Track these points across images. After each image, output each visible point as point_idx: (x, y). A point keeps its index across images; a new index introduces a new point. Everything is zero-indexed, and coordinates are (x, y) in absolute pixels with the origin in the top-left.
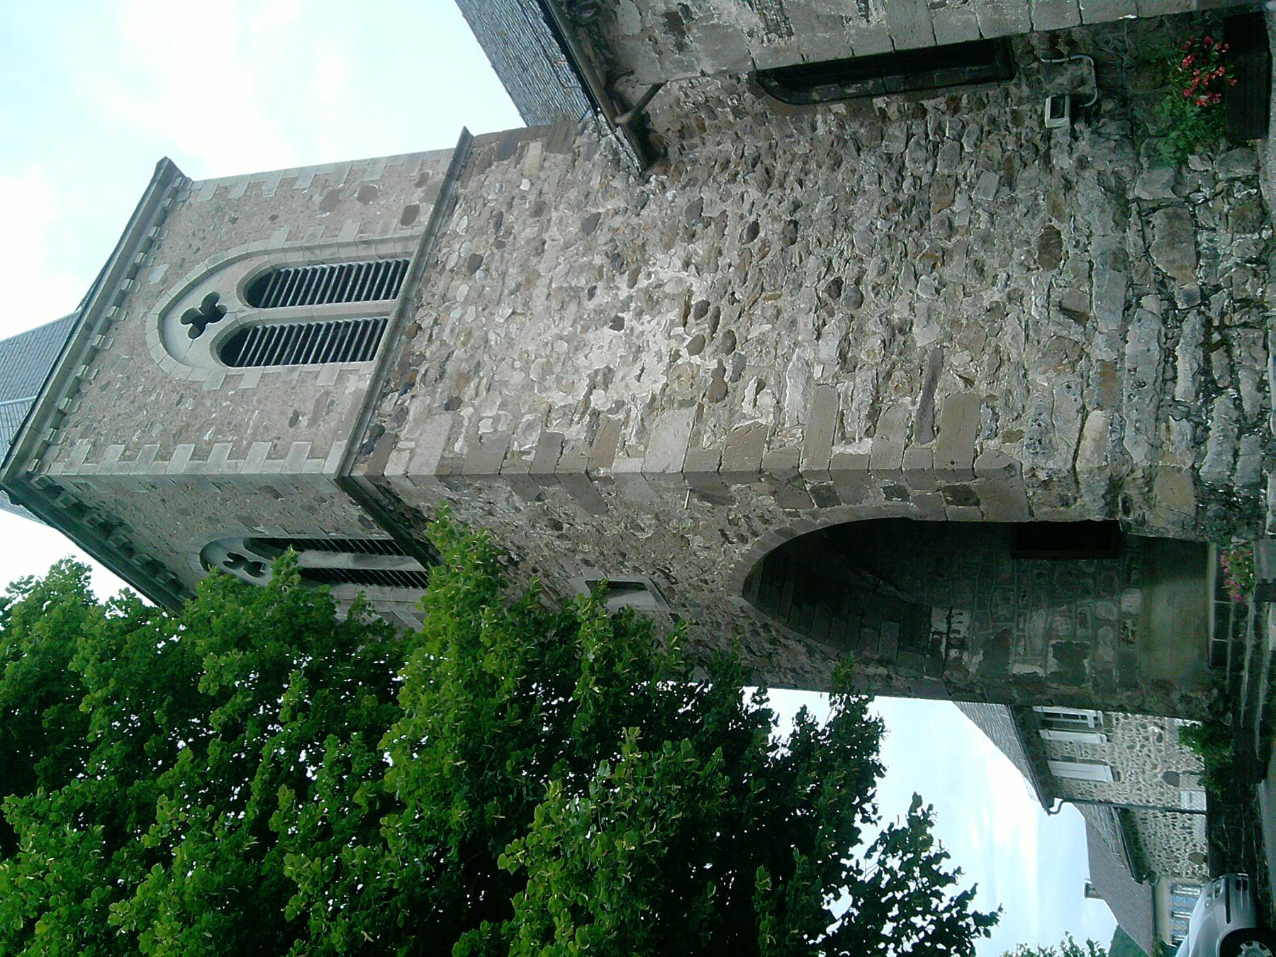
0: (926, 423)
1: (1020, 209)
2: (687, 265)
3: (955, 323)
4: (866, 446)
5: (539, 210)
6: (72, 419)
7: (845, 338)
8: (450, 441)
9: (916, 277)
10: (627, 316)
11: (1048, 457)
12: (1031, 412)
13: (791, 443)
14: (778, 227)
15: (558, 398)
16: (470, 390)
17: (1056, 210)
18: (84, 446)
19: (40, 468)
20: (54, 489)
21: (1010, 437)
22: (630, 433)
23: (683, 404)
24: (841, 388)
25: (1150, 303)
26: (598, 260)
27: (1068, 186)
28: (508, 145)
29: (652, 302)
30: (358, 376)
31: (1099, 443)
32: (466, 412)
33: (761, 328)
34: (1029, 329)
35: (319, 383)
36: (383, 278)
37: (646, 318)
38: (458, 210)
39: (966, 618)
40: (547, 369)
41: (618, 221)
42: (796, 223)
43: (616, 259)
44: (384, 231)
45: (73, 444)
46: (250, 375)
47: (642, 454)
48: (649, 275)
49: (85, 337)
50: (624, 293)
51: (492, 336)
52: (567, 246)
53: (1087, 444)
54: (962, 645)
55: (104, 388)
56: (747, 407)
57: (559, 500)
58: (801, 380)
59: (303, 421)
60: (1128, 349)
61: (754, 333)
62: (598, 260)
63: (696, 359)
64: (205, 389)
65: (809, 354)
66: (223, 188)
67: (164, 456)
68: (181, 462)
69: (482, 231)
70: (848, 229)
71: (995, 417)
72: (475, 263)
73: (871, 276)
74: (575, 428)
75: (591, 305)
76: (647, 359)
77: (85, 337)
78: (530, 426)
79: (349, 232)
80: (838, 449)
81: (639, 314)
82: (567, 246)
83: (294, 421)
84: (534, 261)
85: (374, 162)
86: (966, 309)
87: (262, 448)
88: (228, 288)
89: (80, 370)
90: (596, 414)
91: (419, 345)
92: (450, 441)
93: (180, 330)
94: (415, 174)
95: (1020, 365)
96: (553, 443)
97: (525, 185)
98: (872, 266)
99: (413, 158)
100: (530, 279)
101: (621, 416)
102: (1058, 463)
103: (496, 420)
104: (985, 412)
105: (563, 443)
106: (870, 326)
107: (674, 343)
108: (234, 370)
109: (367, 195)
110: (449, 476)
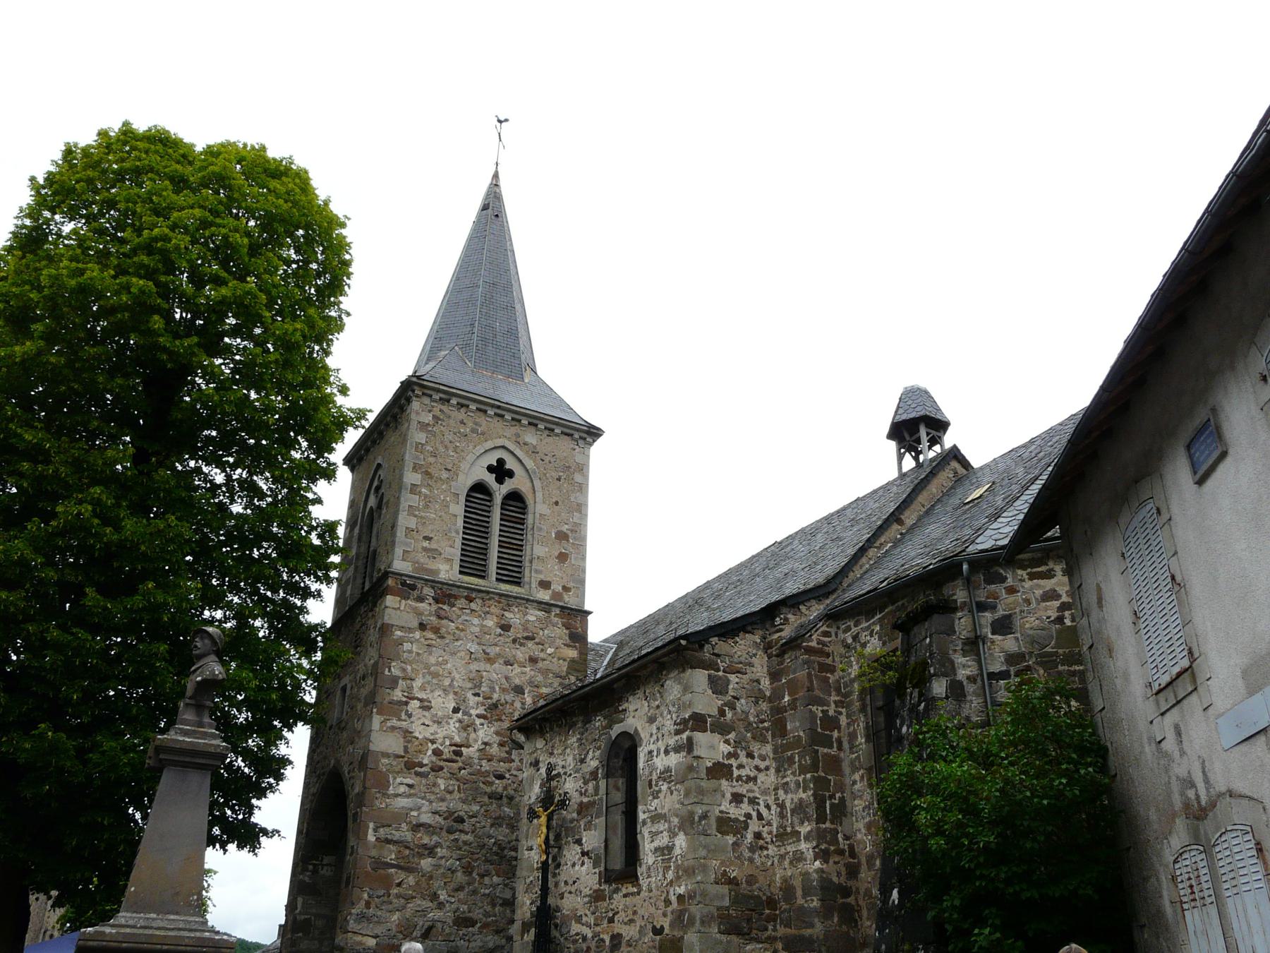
0: (380, 864)
1: (489, 908)
2: (486, 744)
3: (431, 878)
4: (371, 838)
5: (533, 660)
6: (445, 408)
7: (430, 826)
8: (402, 628)
9: (459, 860)
10: (460, 715)
11: (355, 921)
12: (379, 913)
13: (377, 803)
14: (500, 790)
15: (417, 684)
16: (430, 635)
17: (485, 926)
18: (428, 418)
19: (417, 396)
20: (409, 400)
21: (368, 905)
22: (394, 722)
23: (406, 750)
24: (404, 825)
26: (496, 696)
27: (497, 932)
28: (578, 638)
29: (466, 727)
30: (448, 571)
31: (360, 943)
32: (417, 634)
33: (442, 783)
34: (423, 912)
36: (512, 572)
37: (457, 725)
38: (540, 613)
39: (329, 873)
40: (435, 675)
41: (518, 705)
42: (501, 797)
43: (495, 706)
44: (537, 571)
46: (458, 509)
47: (381, 728)
49: (493, 406)
50: (473, 712)
51: (458, 643)
52: (507, 678)
53: (359, 938)
54: (315, 872)
55: (462, 422)
56: (398, 780)
57: (370, 681)
58: (411, 806)
59: (426, 544)
61: (440, 781)
62: (496, 696)
63: (430, 752)
64: (453, 483)
65: (424, 809)
66: (583, 468)
67: (416, 468)
68: (411, 477)
69: (526, 629)
70: (492, 825)
71: (378, 897)
72: (506, 628)
73: (464, 837)
74: (400, 694)
75: (469, 695)
76: (434, 728)
77: (493, 406)
78: (404, 670)
79: (539, 550)
80: (371, 825)
81: (460, 721)
82: (507, 678)
84: (501, 661)
85: (584, 558)
86: (436, 884)
87: (412, 523)
89: (473, 407)
90: (406, 703)
91: (461, 603)
92: (402, 628)
94: (571, 585)
95: (404, 907)
96: (394, 682)
97: (550, 651)
98: (469, 837)
99: (582, 582)
100: (490, 660)
101: (403, 717)
102: (352, 925)
103: (410, 652)
104: (382, 892)
105: (393, 688)
106: (435, 838)
108: (462, 499)
109: (562, 557)
110: (385, 630)
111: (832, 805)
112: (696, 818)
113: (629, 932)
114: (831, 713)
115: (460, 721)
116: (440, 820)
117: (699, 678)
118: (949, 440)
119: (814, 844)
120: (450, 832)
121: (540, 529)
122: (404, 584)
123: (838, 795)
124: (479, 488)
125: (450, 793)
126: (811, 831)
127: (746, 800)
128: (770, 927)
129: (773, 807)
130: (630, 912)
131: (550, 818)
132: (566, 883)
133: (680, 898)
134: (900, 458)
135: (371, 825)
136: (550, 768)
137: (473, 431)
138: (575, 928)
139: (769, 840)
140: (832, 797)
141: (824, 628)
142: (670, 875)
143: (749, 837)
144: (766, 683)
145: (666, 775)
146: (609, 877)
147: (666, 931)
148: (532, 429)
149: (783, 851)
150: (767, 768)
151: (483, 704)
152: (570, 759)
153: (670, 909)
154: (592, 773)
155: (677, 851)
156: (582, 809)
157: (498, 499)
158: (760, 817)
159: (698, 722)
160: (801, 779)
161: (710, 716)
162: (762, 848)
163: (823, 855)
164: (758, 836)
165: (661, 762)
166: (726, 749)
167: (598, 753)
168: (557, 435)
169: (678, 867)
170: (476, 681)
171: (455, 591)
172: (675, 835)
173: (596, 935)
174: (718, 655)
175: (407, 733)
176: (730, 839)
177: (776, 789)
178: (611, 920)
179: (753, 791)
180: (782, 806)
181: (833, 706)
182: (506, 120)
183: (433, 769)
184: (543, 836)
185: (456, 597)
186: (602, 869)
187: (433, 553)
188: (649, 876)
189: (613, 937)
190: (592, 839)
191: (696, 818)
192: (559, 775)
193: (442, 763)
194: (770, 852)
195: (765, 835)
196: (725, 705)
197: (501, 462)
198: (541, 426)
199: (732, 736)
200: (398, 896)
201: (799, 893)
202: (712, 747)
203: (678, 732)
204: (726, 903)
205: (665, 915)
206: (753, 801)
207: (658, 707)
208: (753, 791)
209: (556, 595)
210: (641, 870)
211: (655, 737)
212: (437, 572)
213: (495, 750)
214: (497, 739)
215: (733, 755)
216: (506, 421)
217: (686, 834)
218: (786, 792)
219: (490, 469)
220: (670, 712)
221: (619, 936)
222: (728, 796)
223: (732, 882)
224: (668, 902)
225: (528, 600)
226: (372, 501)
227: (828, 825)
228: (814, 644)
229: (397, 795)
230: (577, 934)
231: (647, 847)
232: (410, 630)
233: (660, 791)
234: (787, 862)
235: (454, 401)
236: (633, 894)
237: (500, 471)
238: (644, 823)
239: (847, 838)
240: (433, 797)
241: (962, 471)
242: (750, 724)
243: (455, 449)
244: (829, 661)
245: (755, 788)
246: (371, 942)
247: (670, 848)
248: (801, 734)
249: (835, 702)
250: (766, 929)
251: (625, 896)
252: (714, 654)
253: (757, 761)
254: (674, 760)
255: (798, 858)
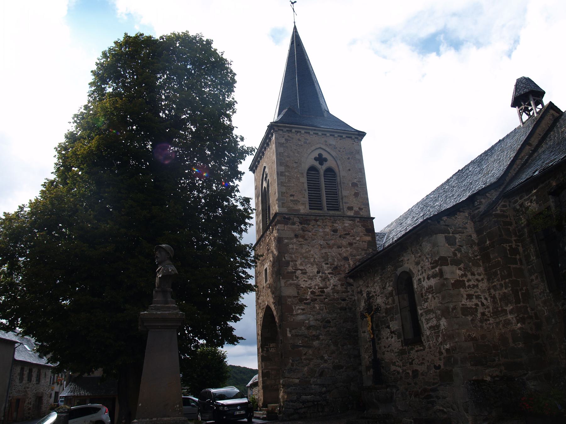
2: (334, 286)
4: (289, 335)
5: (350, 244)
6: (290, 135)
7: (315, 326)
8: (287, 238)
9: (331, 340)
10: (320, 274)
13: (289, 319)
14: (345, 306)
15: (298, 263)
16: (301, 240)
21: (292, 365)
22: (291, 281)
23: (298, 292)
24: (303, 327)
25: (324, 389)
26: (336, 263)
29: (324, 279)
30: (304, 209)
32: (295, 240)
33: (317, 306)
35: (302, 199)
36: (334, 205)
39: (274, 351)
40: (306, 258)
41: (347, 266)
42: (346, 309)
43: (336, 268)
44: (346, 203)
45: (283, 137)
46: (304, 180)
48: (332, 277)
50: (326, 272)
52: (340, 254)
53: (291, 380)
54: (267, 351)
55: (299, 140)
56: (297, 307)
59: (292, 198)
60: (313, 386)
61: (316, 305)
62: (336, 263)
63: (309, 293)
65: (311, 319)
70: (344, 322)
72: (335, 231)
73: (331, 329)
74: (291, 268)
75: (323, 264)
76: (309, 282)
77: (312, 130)
78: (291, 257)
79: (345, 193)
80: (288, 329)
81: (321, 277)
82: (340, 254)
83: (292, 195)
84: (336, 247)
88: (330, 163)
90: (295, 272)
92: (287, 238)
93: (315, 154)
94: (363, 207)
96: (287, 263)
97: (358, 239)
98: (334, 329)
100: (330, 247)
101: (295, 279)
103: (293, 249)
105: (288, 266)
106: (318, 331)
107: (313, 287)
108: (305, 175)
111: (522, 294)
112: (451, 310)
113: (422, 369)
114: (514, 246)
115: (321, 277)
116: (319, 323)
117: (441, 238)
118: (546, 101)
119: (516, 315)
120: (324, 328)
121: (344, 183)
122: (285, 218)
123: (524, 288)
124: (312, 169)
125: (322, 310)
126: (512, 309)
127: (474, 297)
128: (497, 359)
129: (489, 299)
130: (421, 359)
131: (372, 318)
132: (385, 347)
133: (447, 350)
134: (520, 115)
135: (288, 329)
136: (368, 293)
137: (305, 143)
138: (393, 368)
139: (489, 315)
140: (521, 289)
141: (503, 203)
142: (440, 339)
143: (479, 315)
144: (474, 236)
145: (430, 289)
146: (406, 342)
147: (442, 367)
148: (332, 137)
149: (498, 320)
150: (482, 280)
151: (330, 268)
152: (377, 288)
153: (442, 356)
154: (389, 293)
155: (442, 327)
156: (387, 311)
157: (322, 172)
158: (483, 304)
159: (443, 261)
160: (503, 282)
161: (449, 257)
162: (486, 320)
163: (521, 320)
164: (483, 314)
165: (426, 284)
166: (459, 272)
167: (391, 283)
168: (344, 138)
169: (443, 335)
170: (325, 257)
171: (309, 217)
172: (440, 319)
173: (404, 371)
174: (448, 226)
175: (298, 286)
176: (470, 318)
177: (489, 289)
178: (411, 363)
179: (477, 292)
180: (494, 297)
181: (514, 242)
182: (295, 2)
183: (312, 300)
184: (370, 327)
185: (310, 220)
186: (402, 339)
187: (296, 202)
188: (428, 341)
189: (413, 372)
190: (395, 325)
191: (451, 310)
192: (373, 296)
193: (316, 297)
194: (491, 322)
195: (487, 313)
196: (456, 250)
197: (320, 155)
198: (336, 135)
199: (462, 266)
200: (305, 359)
201: (510, 341)
202: (453, 273)
203: (433, 268)
204: (472, 350)
205: (440, 359)
206: (478, 297)
207: (420, 256)
208: (477, 292)
209: (356, 212)
210: (424, 338)
211: (421, 272)
212: (299, 210)
213: (339, 288)
214: (340, 283)
215: (465, 275)
216: (320, 136)
217: (446, 318)
218: (495, 290)
219: (316, 159)
220: (427, 258)
221: (417, 370)
222: (465, 296)
223: (473, 339)
224: (441, 353)
225: (343, 217)
226: (265, 185)
227: (522, 304)
228: (498, 212)
229: (298, 314)
230: (394, 371)
231: (425, 327)
232: (291, 239)
233: (428, 298)
234: (501, 326)
235: (293, 130)
236: (421, 350)
237: (321, 159)
238: (422, 315)
239: (532, 309)
240: (314, 313)
241: (557, 115)
242: (470, 258)
243: (298, 152)
244: (508, 220)
245: (478, 290)
246: (297, 381)
247: (438, 326)
248: (500, 259)
249: (515, 240)
250: (494, 360)
251: (417, 351)
252: (446, 225)
253: (477, 277)
254: (433, 282)
255: (507, 323)
